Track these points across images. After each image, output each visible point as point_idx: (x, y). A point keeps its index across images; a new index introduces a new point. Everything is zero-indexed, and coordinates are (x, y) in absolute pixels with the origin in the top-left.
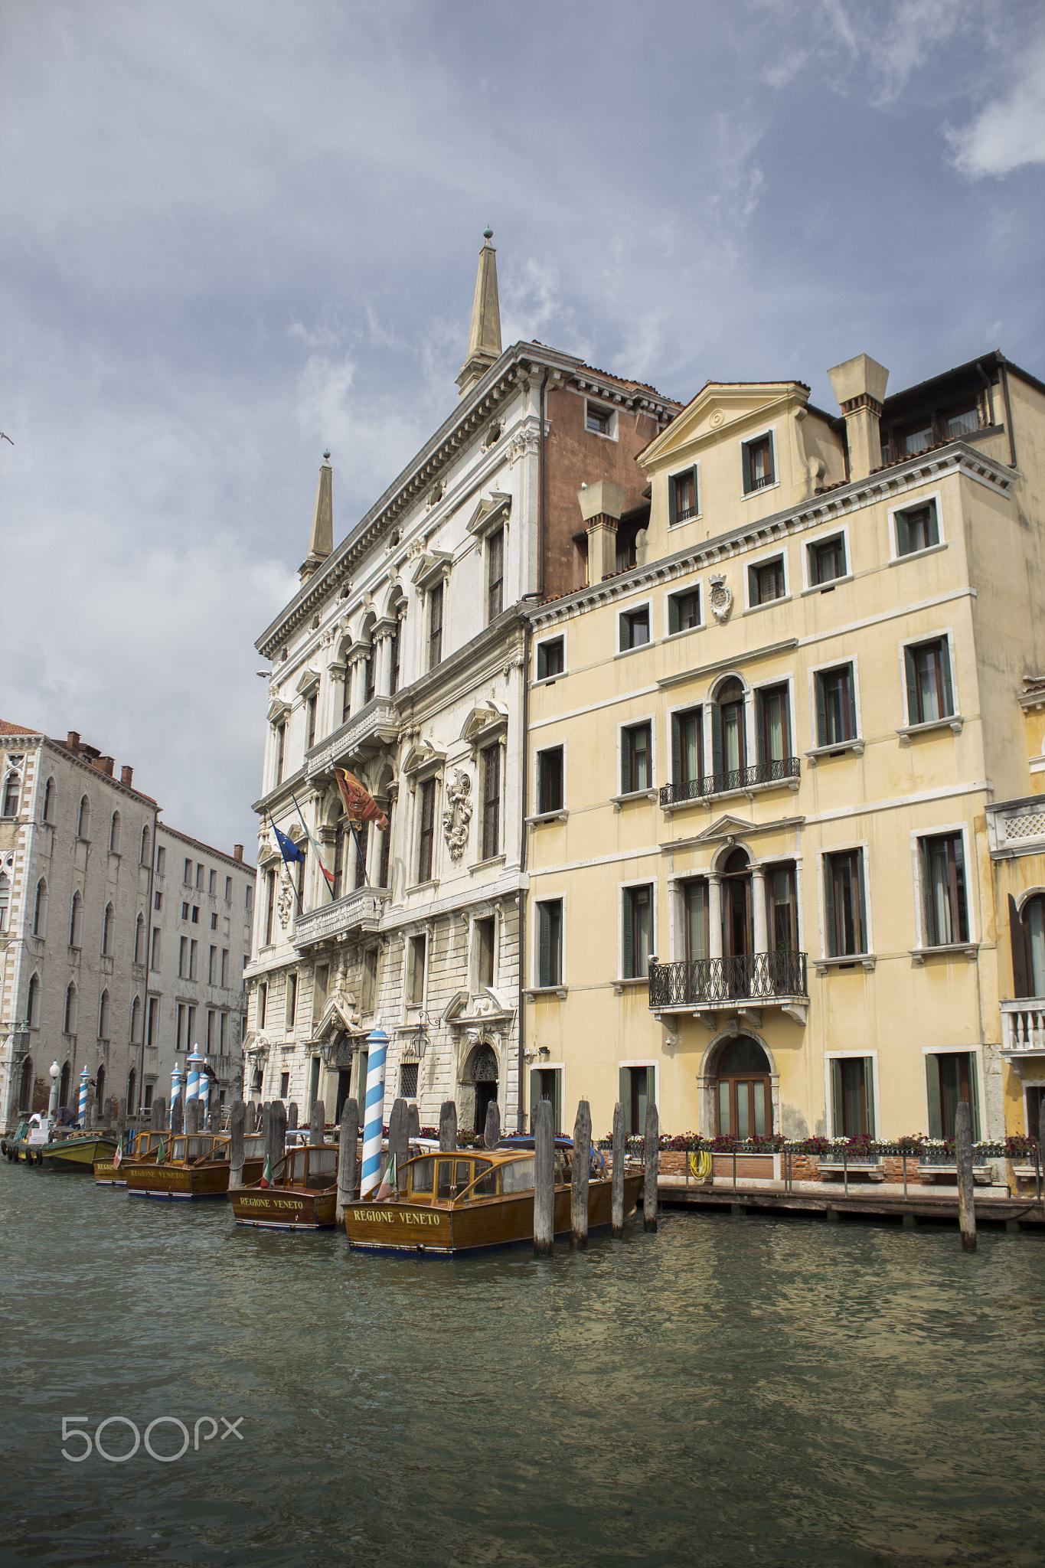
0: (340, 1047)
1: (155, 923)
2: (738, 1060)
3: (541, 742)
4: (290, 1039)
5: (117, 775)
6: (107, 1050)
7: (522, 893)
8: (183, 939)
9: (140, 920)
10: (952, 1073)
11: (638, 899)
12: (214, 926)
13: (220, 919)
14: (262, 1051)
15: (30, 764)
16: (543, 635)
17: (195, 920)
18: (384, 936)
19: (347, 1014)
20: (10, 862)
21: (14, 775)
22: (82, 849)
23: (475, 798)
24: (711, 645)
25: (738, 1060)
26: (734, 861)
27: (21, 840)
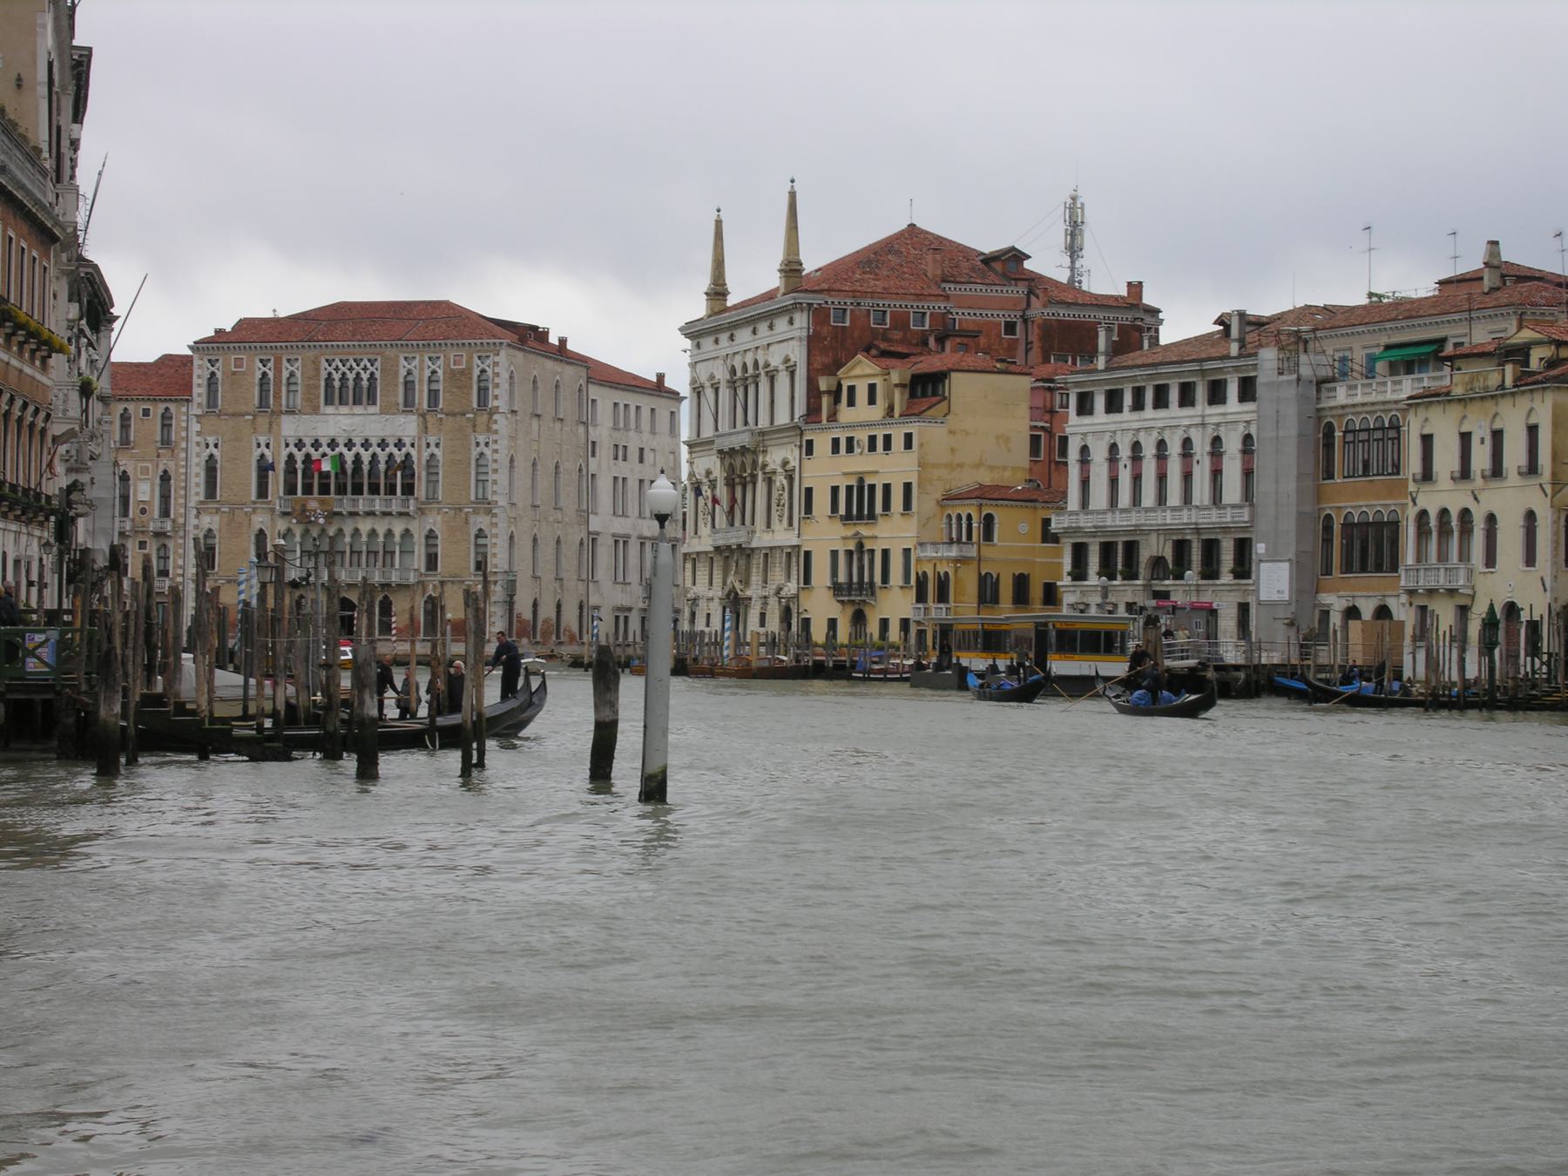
0: (735, 604)
1: (591, 471)
2: (859, 618)
3: (806, 485)
4: (710, 594)
6: (562, 587)
7: (799, 546)
9: (580, 470)
10: (905, 623)
12: (641, 460)
14: (695, 601)
15: (496, 364)
16: (806, 438)
19: (738, 586)
20: (487, 444)
21: (483, 371)
23: (786, 495)
25: (859, 618)
26: (860, 546)
27: (495, 427)
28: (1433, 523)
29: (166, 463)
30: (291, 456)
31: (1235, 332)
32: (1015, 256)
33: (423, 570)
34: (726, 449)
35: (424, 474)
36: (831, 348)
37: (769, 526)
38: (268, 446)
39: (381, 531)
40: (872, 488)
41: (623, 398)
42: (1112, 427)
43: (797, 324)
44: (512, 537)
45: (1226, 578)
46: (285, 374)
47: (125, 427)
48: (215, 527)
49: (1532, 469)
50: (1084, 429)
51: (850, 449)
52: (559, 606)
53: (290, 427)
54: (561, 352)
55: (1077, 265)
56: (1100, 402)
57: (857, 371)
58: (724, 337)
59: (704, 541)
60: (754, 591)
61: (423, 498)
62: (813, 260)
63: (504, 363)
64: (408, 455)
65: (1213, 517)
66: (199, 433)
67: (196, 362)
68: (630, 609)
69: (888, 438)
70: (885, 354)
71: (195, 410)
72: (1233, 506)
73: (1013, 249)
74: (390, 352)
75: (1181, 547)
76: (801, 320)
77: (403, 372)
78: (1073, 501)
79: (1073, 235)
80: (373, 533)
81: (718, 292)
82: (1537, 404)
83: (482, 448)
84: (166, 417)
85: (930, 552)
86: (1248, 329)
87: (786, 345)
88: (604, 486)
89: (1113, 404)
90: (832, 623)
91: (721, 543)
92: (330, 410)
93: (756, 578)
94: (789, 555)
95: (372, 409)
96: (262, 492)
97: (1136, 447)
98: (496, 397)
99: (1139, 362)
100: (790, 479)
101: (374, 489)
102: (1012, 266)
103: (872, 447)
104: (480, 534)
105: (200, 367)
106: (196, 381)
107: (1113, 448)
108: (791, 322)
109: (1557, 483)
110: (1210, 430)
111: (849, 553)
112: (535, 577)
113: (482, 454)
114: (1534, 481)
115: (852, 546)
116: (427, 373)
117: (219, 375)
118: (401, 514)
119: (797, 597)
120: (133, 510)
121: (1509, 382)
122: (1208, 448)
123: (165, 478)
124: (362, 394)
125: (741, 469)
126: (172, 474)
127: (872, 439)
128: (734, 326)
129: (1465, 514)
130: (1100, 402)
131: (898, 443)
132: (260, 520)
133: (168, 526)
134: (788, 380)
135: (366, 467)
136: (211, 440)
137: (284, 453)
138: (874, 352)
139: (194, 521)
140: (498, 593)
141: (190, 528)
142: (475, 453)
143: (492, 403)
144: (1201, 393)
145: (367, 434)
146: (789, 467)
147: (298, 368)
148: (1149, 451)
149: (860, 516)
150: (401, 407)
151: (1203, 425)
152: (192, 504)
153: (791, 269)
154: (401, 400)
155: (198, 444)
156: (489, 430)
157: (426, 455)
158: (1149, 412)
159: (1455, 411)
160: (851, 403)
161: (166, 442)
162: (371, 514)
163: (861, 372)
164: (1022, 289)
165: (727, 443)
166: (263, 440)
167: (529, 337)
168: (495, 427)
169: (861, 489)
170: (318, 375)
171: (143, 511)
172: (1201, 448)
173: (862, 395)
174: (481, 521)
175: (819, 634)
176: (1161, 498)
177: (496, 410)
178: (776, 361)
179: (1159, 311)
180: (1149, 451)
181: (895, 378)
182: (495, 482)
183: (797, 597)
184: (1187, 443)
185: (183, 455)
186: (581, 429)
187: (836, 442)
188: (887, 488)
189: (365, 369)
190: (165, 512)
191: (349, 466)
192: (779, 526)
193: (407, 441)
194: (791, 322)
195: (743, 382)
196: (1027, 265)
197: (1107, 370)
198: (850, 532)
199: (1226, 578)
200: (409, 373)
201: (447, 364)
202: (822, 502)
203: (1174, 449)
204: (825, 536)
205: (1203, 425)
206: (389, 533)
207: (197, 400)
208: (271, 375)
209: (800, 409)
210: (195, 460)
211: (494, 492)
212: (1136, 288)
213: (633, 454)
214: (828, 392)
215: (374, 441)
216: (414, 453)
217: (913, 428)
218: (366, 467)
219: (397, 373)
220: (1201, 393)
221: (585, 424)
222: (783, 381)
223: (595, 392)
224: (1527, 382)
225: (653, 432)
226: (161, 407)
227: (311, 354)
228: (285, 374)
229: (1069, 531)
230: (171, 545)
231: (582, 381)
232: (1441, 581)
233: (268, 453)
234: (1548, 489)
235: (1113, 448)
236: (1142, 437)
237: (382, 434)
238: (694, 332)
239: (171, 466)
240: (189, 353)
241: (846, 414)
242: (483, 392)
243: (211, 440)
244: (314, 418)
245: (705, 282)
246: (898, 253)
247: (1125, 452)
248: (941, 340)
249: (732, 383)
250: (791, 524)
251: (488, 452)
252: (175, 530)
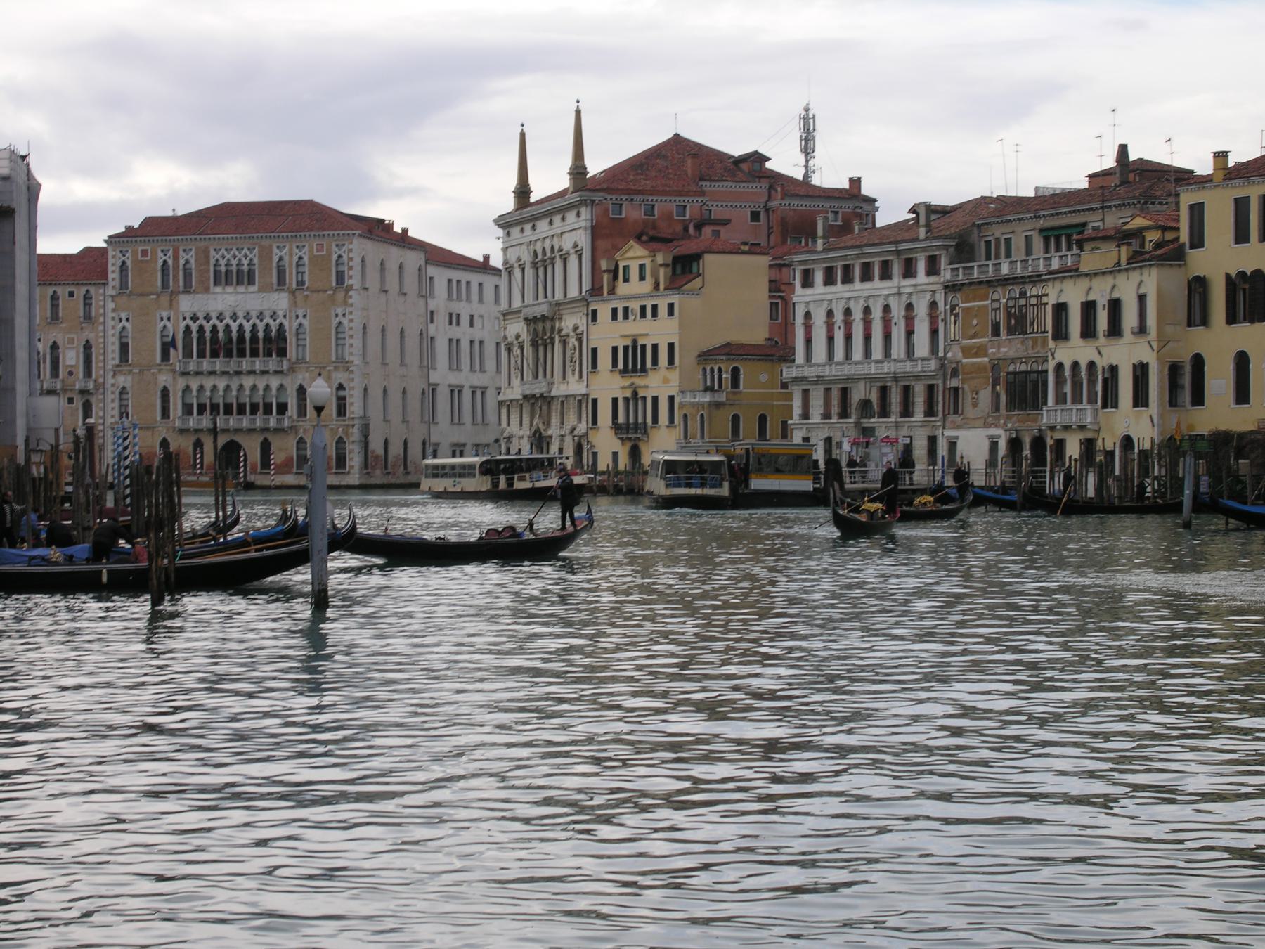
3: (592, 345)
4: (521, 433)
5: (397, 229)
7: (587, 395)
8: (450, 340)
11: (615, 401)
12: (472, 325)
13: (476, 318)
14: (509, 439)
15: (350, 251)
16: (592, 307)
17: (458, 324)
18: (552, 398)
19: (541, 426)
21: (340, 256)
22: (383, 295)
24: (634, 327)
26: (635, 394)
27: (350, 301)
28: (1067, 373)
29: (88, 334)
30: (188, 328)
31: (922, 221)
32: (757, 159)
33: (295, 417)
34: (530, 317)
35: (294, 340)
36: (607, 234)
37: (564, 378)
38: (169, 319)
39: (261, 386)
40: (643, 347)
41: (456, 275)
42: (829, 297)
43: (583, 217)
44: (366, 389)
45: (919, 416)
46: (182, 262)
47: (55, 306)
48: (128, 385)
49: (1142, 330)
50: (807, 299)
51: (626, 317)
52: (405, 443)
53: (187, 304)
54: (403, 240)
55: (811, 163)
56: (819, 277)
57: (631, 254)
58: (528, 227)
59: (515, 392)
60: (554, 431)
61: (294, 359)
62: (595, 166)
63: (358, 248)
64: (281, 325)
65: (908, 367)
66: (114, 310)
67: (111, 253)
68: (464, 445)
69: (655, 308)
70: (653, 239)
71: (111, 292)
72: (923, 359)
73: (756, 152)
74: (265, 243)
75: (884, 391)
76: (585, 213)
77: (276, 259)
78: (800, 357)
79: (807, 140)
80: (254, 388)
81: (523, 191)
82: (1145, 277)
83: (340, 318)
84: (87, 297)
85: (689, 398)
86: (933, 217)
87: (574, 232)
88: (442, 348)
89: (829, 280)
90: (615, 454)
91: (528, 392)
92: (218, 289)
93: (555, 420)
94: (580, 401)
95: (252, 288)
96: (165, 356)
97: (848, 312)
98: (351, 277)
99: (849, 244)
100: (580, 340)
101: (255, 353)
102: (757, 166)
103: (643, 315)
104: (341, 387)
105: (113, 257)
106: (110, 268)
107: (830, 313)
108: (578, 215)
109: (1163, 341)
110: (904, 298)
111: (627, 400)
112: (385, 420)
113: (340, 323)
114: (1145, 339)
115: (628, 394)
116: (295, 259)
117: (129, 263)
118: (276, 372)
119: (586, 434)
120: (62, 372)
121: (1124, 261)
122: (903, 313)
123: (88, 346)
124: (244, 277)
125: (543, 331)
126: (92, 342)
127: (643, 308)
128: (535, 219)
129: (1092, 365)
130: (819, 277)
131: (663, 310)
132: (164, 379)
133: (91, 386)
134: (577, 261)
135: (248, 335)
136: (124, 315)
137: (182, 325)
138: (644, 238)
139: (110, 381)
140: (356, 433)
141: (108, 386)
142: (335, 322)
143: (347, 282)
144: (896, 269)
145: (248, 308)
146: (579, 331)
147: (192, 257)
148: (858, 315)
149: (634, 370)
150: (275, 287)
151: (899, 294)
152: (109, 367)
153: (578, 171)
154: (275, 280)
155: (113, 318)
156: (345, 303)
157: (295, 324)
158: (858, 285)
159: (1084, 283)
160: (626, 280)
161: (88, 317)
162: (252, 372)
163: (634, 255)
164: (764, 185)
165: (530, 312)
166: (165, 314)
167: (378, 229)
168: (350, 301)
169: (635, 348)
170: (208, 262)
171: (71, 373)
172: (898, 313)
173: (634, 273)
174: (340, 377)
175: (604, 463)
176: (868, 353)
177: (350, 288)
178: (567, 244)
179: (875, 200)
180: (858, 315)
181: (660, 259)
182: (351, 345)
183: (586, 434)
184: (887, 309)
185: (101, 328)
186: (422, 301)
187: (615, 311)
188: (655, 347)
189: (246, 256)
190: (88, 373)
191: (234, 335)
192: (572, 379)
193: (280, 313)
194: (578, 215)
195: (543, 263)
196: (768, 165)
197: (825, 250)
198: (627, 382)
199: (919, 416)
200: (281, 259)
201: (311, 251)
202: (605, 359)
203: (877, 314)
204: (608, 386)
205: (899, 294)
206: (267, 388)
207: (111, 283)
208: (170, 262)
209: (586, 285)
210: (111, 332)
211: (351, 354)
212: (855, 182)
213: (465, 321)
214: (608, 271)
215: (254, 314)
216: (286, 323)
217: (675, 299)
218: (248, 335)
219: (271, 258)
220: (896, 269)
221: (425, 297)
222: (573, 262)
223: (432, 271)
224: (1138, 259)
225: (481, 300)
227: (203, 244)
228: (182, 262)
229: (797, 380)
230: (93, 400)
231: (422, 262)
232: (1074, 419)
233: (169, 325)
234: (1155, 345)
235: (830, 313)
236: (852, 305)
237: (259, 308)
238: (505, 223)
239: (91, 336)
240: (105, 245)
241: (622, 288)
242: (340, 277)
243: (124, 315)
244: (205, 296)
245: (512, 181)
246: (665, 157)
247: (839, 317)
248: (698, 227)
249: (535, 265)
250: (581, 376)
251: (345, 321)
252: (97, 387)
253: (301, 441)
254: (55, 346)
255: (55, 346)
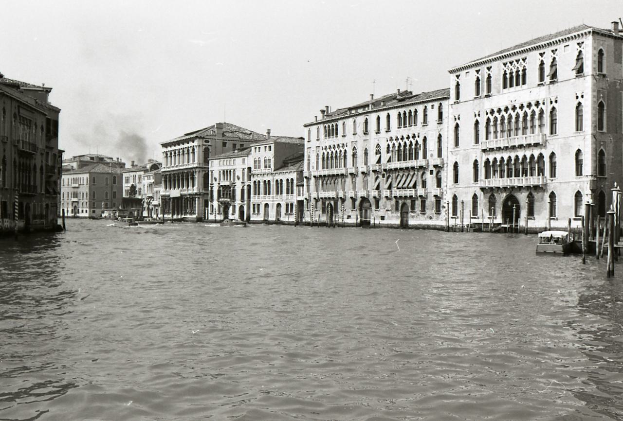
92: (506, 90)
139: (450, 158)
193: (541, 102)
216: (544, 107)
226: (437, 104)
253: (552, 196)
254: (425, 139)
255: (425, 139)
